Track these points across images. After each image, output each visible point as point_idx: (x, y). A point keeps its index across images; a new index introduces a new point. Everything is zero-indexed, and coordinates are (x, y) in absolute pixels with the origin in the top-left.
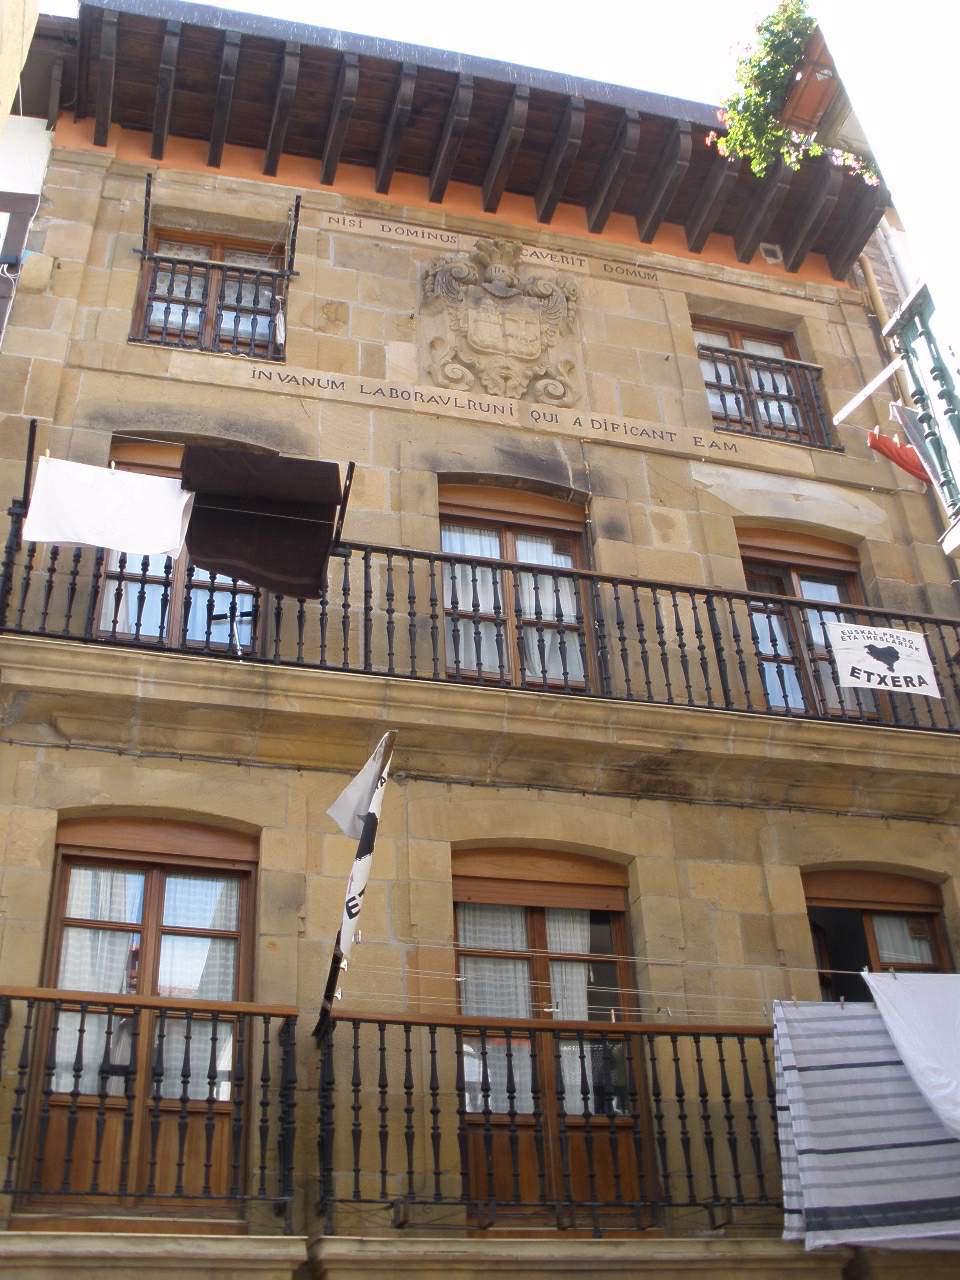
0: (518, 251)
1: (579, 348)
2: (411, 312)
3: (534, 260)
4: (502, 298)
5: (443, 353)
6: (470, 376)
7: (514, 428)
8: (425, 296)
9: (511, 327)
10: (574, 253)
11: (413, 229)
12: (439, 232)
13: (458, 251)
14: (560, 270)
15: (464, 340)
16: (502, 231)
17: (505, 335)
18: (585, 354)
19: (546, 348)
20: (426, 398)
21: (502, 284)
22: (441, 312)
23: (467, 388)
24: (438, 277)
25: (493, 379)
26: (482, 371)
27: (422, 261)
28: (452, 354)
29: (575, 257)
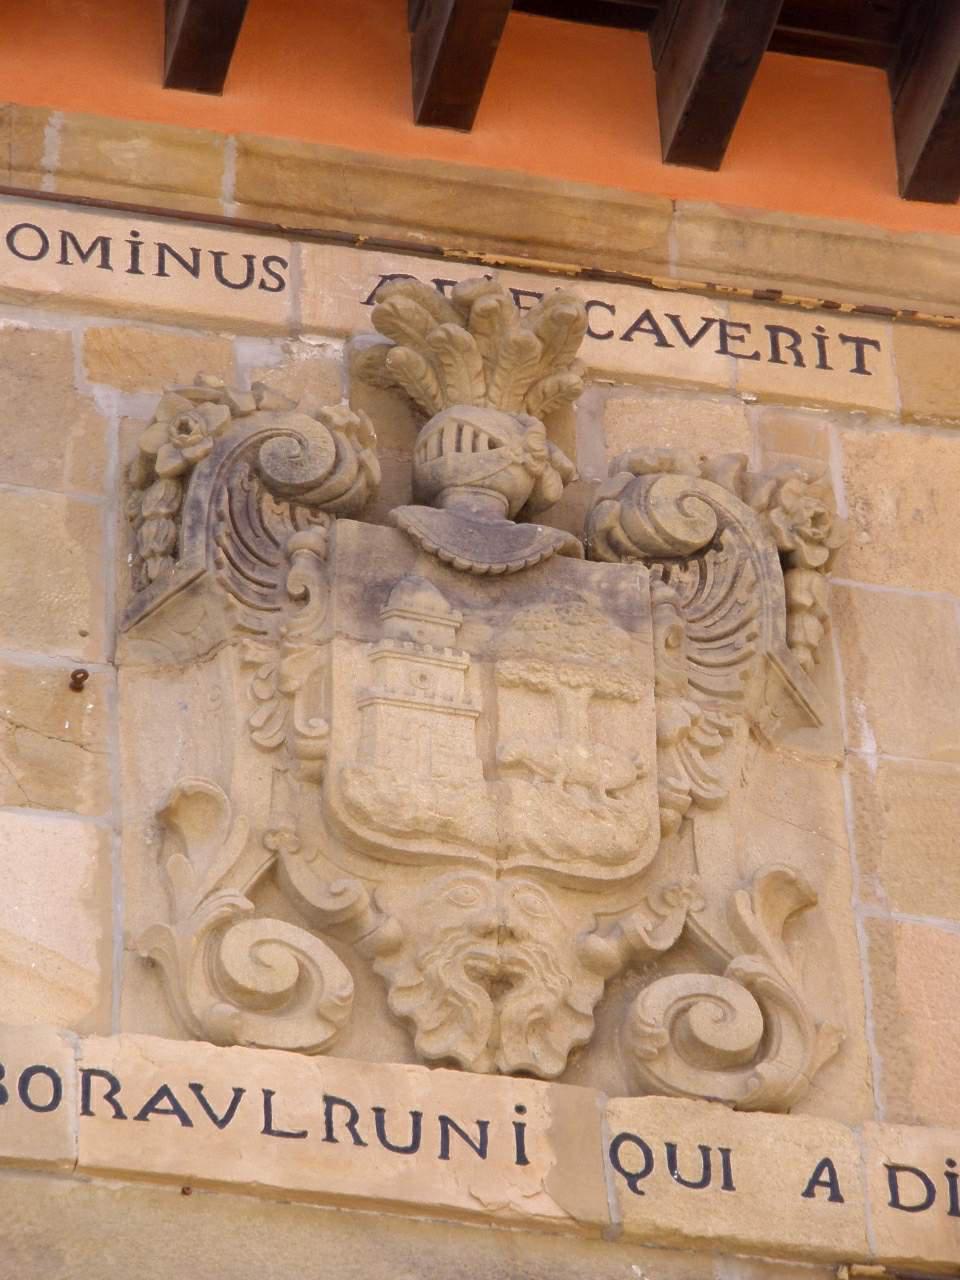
0: (562, 334)
1: (839, 794)
2: (71, 655)
3: (641, 354)
4: (486, 577)
5: (218, 864)
6: (335, 975)
7: (533, 1225)
8: (141, 583)
9: (523, 723)
10: (830, 307)
11: (88, 226)
12: (209, 239)
13: (295, 331)
14: (763, 398)
15: (311, 793)
16: (498, 215)
17: (494, 769)
18: (866, 831)
19: (683, 817)
20: (132, 1100)
21: (495, 503)
22: (209, 654)
23: (317, 1034)
24: (199, 490)
25: (436, 986)
26: (393, 949)
27: (129, 388)
28: (260, 863)
29: (834, 326)
